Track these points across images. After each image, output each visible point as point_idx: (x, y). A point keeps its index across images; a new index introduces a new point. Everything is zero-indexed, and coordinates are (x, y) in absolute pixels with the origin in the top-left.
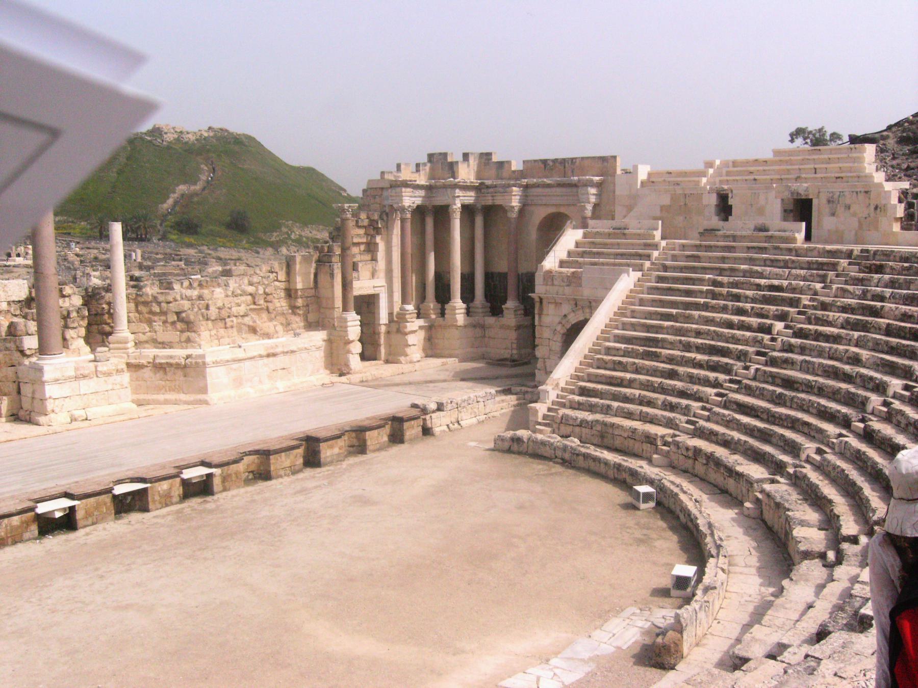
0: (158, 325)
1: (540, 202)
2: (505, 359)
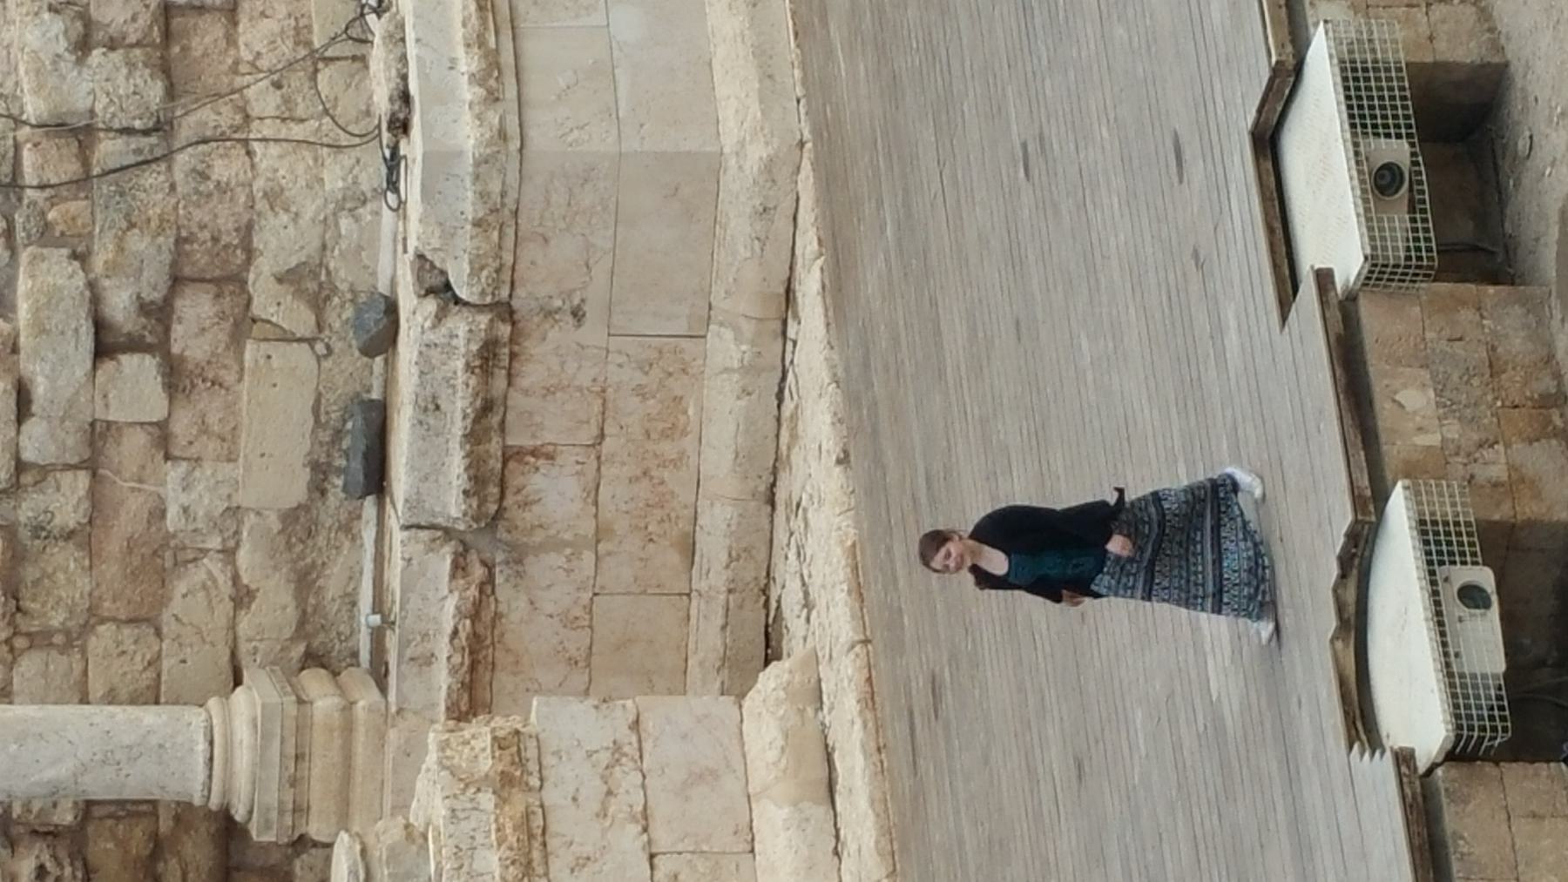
0: (187, 496)
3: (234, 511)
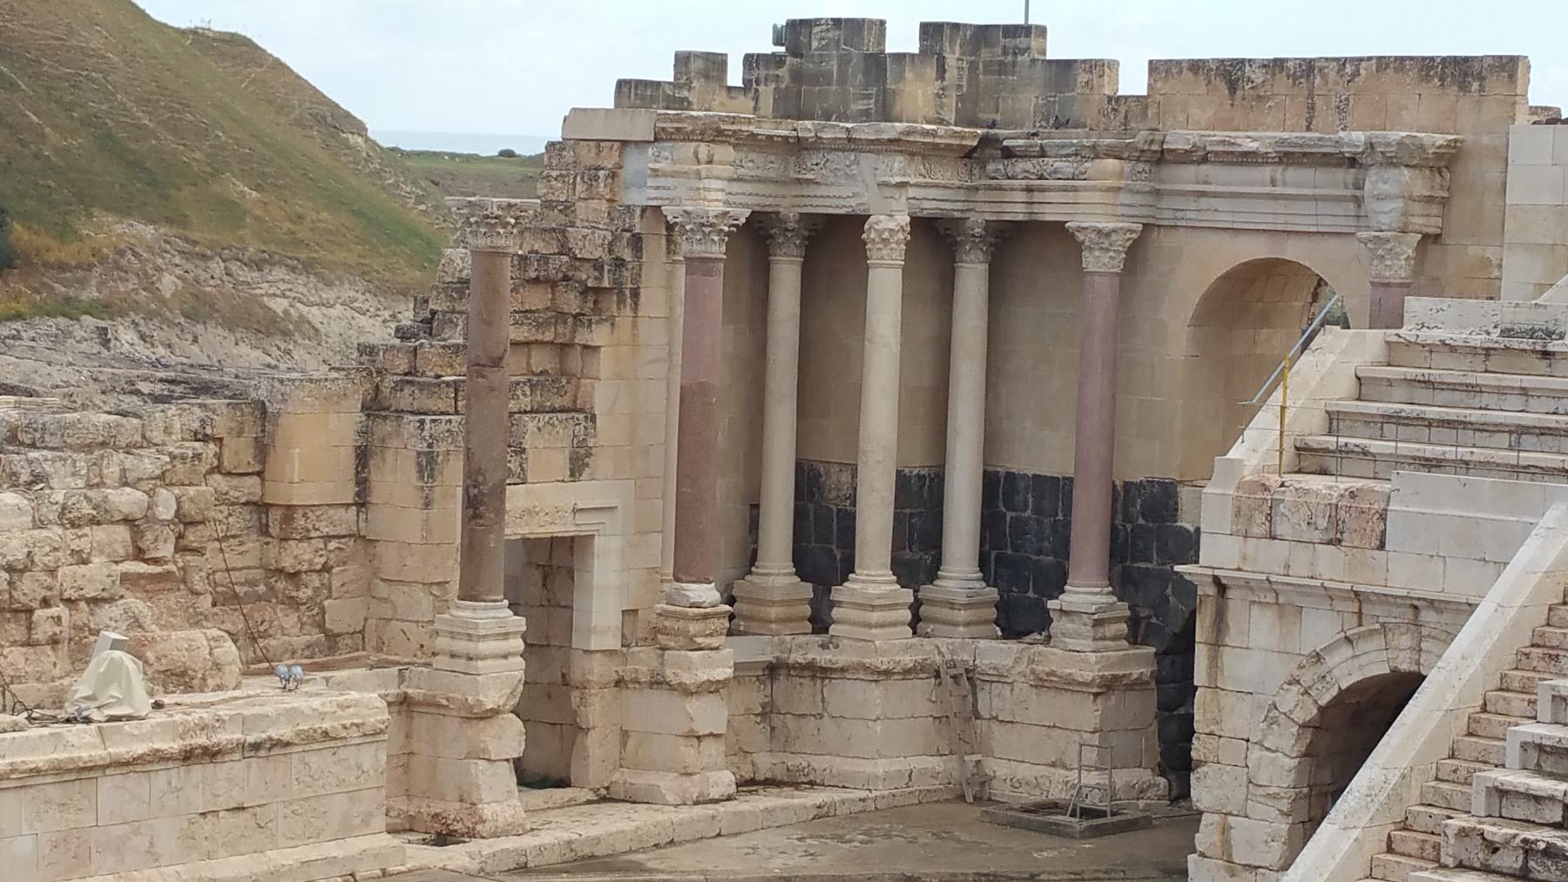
1: (1208, 219)
2: (1054, 807)
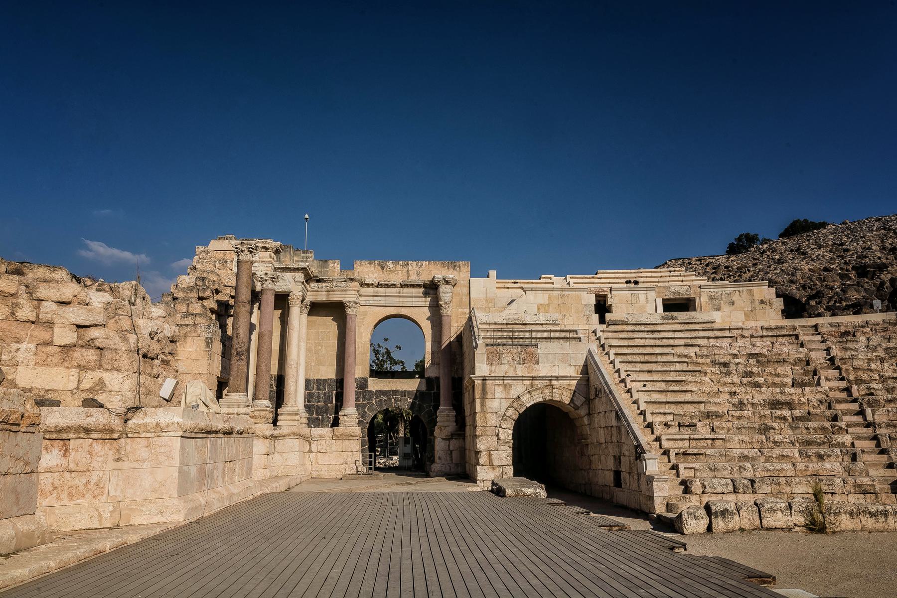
3: (17, 364)
